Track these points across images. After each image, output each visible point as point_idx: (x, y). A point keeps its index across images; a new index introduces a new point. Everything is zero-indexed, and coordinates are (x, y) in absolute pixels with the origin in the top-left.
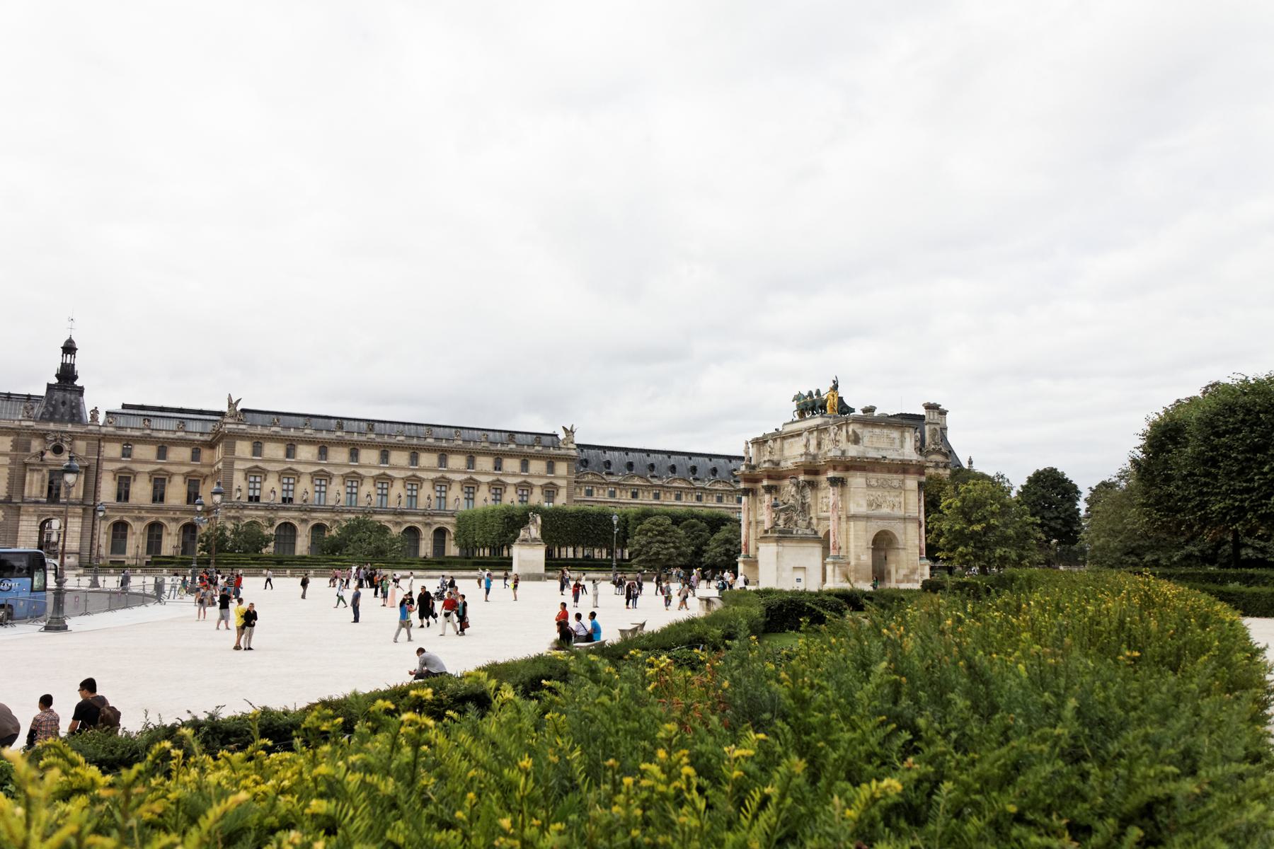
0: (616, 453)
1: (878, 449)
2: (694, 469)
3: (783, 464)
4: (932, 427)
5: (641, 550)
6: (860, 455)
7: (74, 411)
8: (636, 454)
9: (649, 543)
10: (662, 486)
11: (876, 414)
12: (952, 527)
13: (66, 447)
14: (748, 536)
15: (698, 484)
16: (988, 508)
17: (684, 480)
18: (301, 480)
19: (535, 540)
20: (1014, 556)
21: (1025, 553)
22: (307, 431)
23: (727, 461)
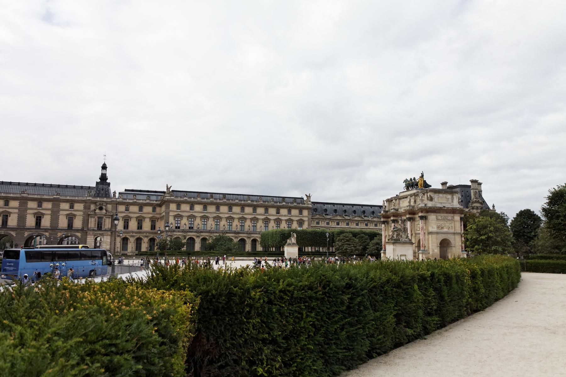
0: (329, 206)
1: (441, 203)
2: (364, 212)
3: (399, 210)
4: (475, 190)
5: (339, 248)
6: (433, 206)
7: (107, 193)
8: (338, 206)
9: (343, 245)
10: (350, 220)
11: (448, 185)
12: (472, 237)
13: (104, 207)
15: (366, 218)
16: (488, 229)
17: (360, 217)
19: (294, 244)
20: (500, 249)
21: (506, 248)
22: (198, 199)
23: (379, 208)
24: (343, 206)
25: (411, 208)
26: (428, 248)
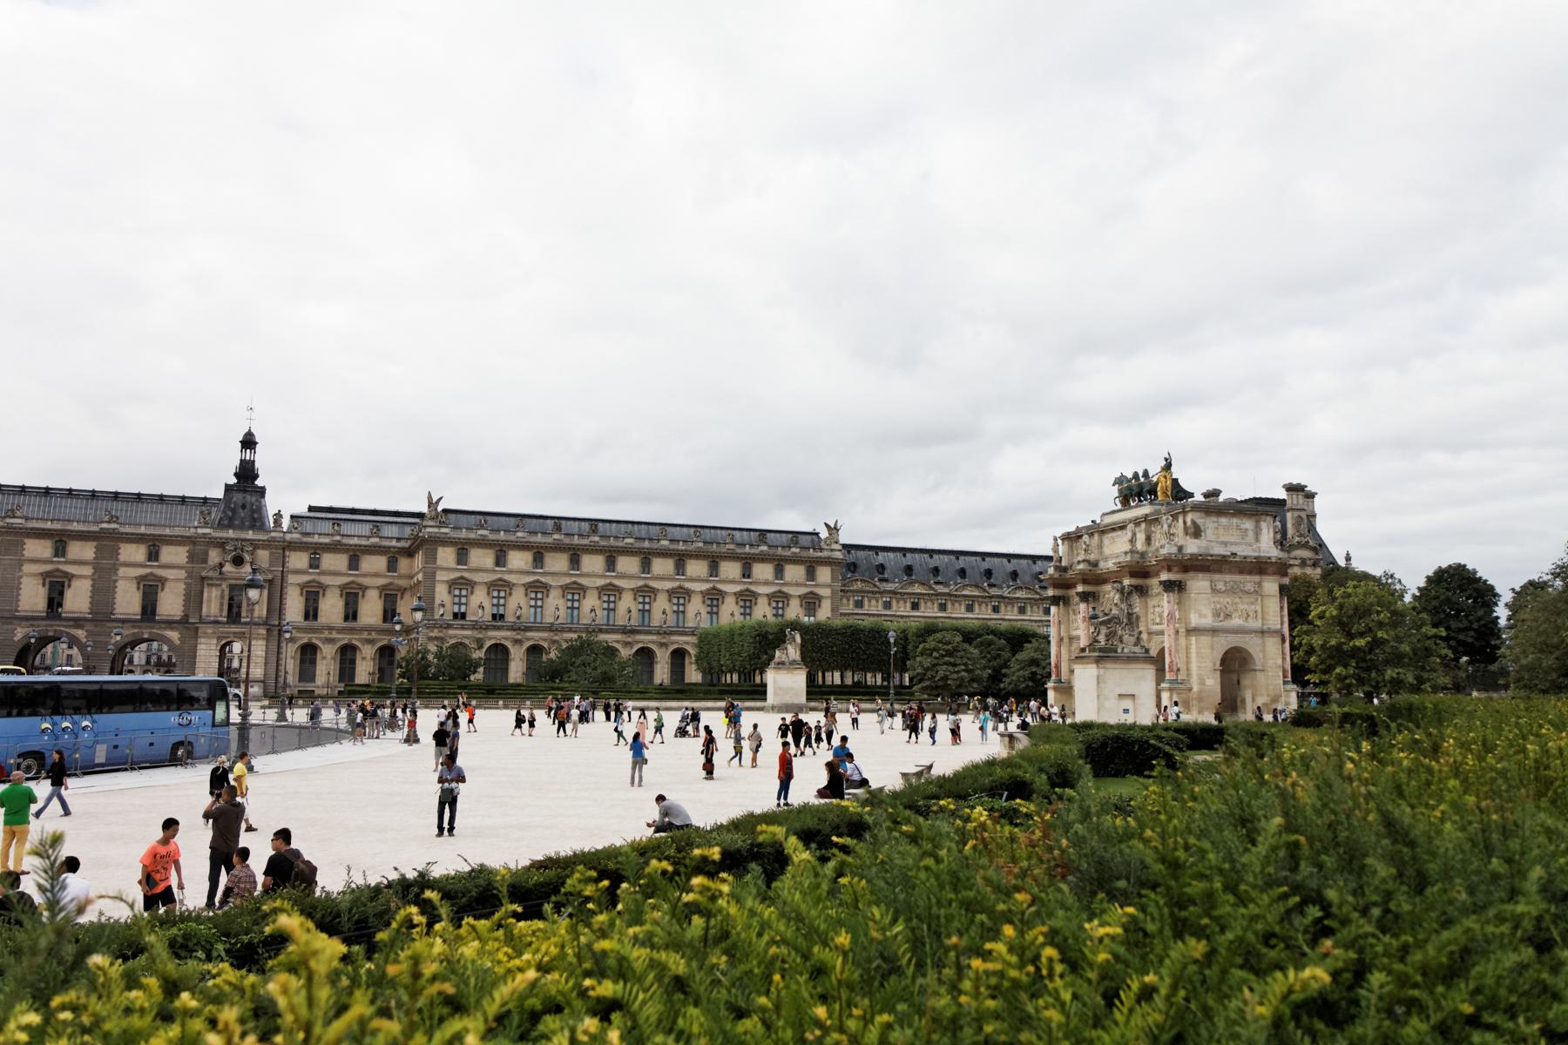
0: (891, 555)
1: (1225, 544)
3: (1102, 564)
6: (1202, 551)
9: (935, 665)
10: (949, 595)
11: (1221, 499)
12: (1325, 642)
13: (247, 557)
14: (1059, 656)
15: (994, 591)
16: (1374, 617)
17: (977, 586)
18: (514, 593)
19: (793, 662)
20: (1410, 679)
21: (1425, 675)
22: (519, 534)
23: (1030, 562)
24: (931, 557)
25: (1137, 557)
26: (1189, 675)
